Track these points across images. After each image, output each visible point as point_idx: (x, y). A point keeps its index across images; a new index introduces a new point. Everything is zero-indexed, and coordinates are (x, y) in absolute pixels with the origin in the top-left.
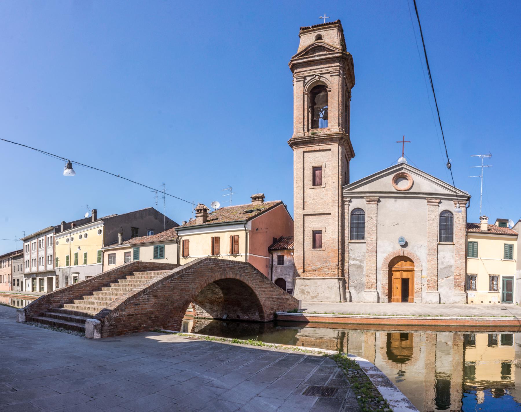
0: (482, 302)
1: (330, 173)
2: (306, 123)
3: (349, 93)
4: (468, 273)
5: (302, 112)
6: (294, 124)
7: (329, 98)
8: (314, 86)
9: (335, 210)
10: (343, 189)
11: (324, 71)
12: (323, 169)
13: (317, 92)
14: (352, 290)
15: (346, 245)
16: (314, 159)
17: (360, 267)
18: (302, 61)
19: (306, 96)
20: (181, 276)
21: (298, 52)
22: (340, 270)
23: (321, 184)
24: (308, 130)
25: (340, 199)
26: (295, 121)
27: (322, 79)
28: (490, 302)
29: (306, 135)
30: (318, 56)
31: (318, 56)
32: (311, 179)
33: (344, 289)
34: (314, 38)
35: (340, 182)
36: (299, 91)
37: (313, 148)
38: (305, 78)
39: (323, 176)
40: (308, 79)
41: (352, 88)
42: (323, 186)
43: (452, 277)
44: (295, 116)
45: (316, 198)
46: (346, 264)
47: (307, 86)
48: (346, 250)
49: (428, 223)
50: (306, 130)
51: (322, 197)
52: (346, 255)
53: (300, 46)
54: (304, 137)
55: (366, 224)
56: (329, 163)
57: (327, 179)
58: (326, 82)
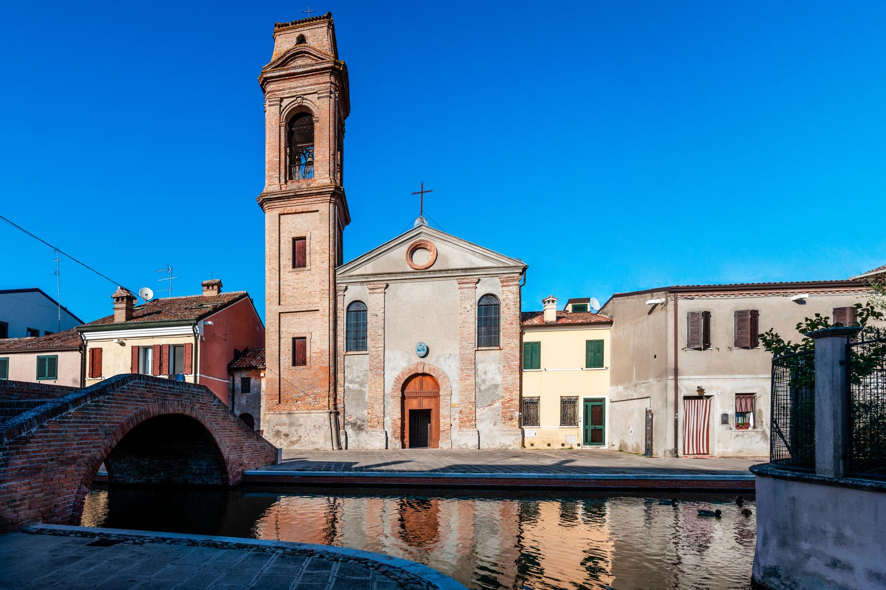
0: (549, 445)
1: (318, 248)
2: (283, 171)
3: (343, 125)
4: (524, 395)
5: (277, 154)
6: (266, 172)
7: (315, 132)
8: (295, 113)
9: (324, 305)
10: (335, 271)
11: (309, 89)
12: (308, 241)
13: (299, 124)
14: (350, 431)
15: (340, 359)
16: (295, 225)
17: (361, 393)
18: (278, 74)
19: (283, 128)
20: (83, 409)
21: (272, 60)
22: (332, 399)
23: (304, 266)
24: (286, 182)
25: (332, 287)
26: (267, 167)
27: (306, 103)
28: (563, 445)
29: (283, 189)
30: (300, 67)
31: (300, 67)
32: (291, 256)
33: (338, 429)
34: (295, 41)
35: (332, 262)
36: (273, 119)
37: (294, 209)
38: (281, 100)
39: (307, 252)
40: (285, 102)
41: (345, 118)
42: (308, 267)
43: (498, 404)
44: (267, 160)
45: (297, 286)
46: (340, 389)
47: (285, 114)
48: (340, 367)
49: (460, 317)
50: (283, 181)
51: (306, 285)
52: (340, 376)
53: (274, 53)
54: (281, 192)
55: (369, 326)
56: (315, 231)
57: (313, 257)
58: (312, 108)
